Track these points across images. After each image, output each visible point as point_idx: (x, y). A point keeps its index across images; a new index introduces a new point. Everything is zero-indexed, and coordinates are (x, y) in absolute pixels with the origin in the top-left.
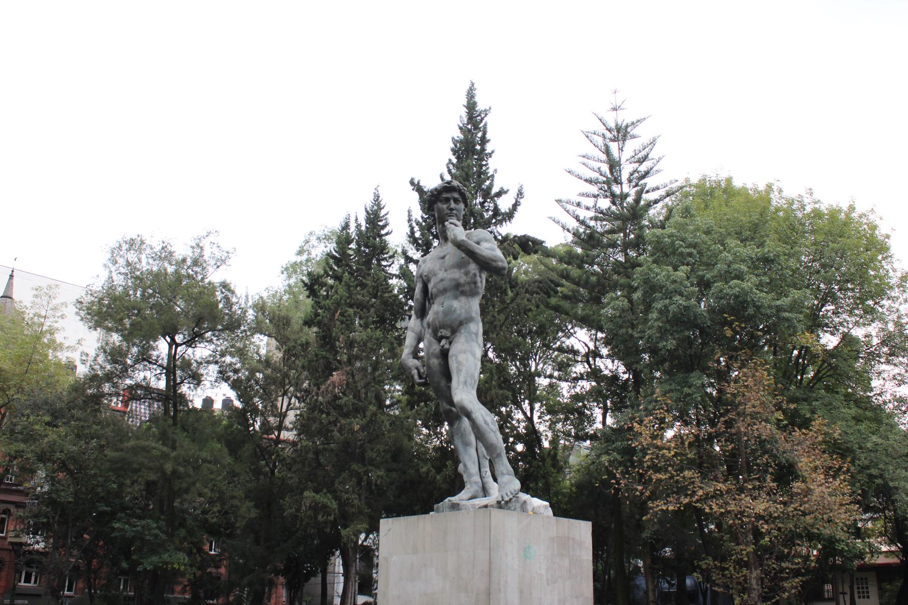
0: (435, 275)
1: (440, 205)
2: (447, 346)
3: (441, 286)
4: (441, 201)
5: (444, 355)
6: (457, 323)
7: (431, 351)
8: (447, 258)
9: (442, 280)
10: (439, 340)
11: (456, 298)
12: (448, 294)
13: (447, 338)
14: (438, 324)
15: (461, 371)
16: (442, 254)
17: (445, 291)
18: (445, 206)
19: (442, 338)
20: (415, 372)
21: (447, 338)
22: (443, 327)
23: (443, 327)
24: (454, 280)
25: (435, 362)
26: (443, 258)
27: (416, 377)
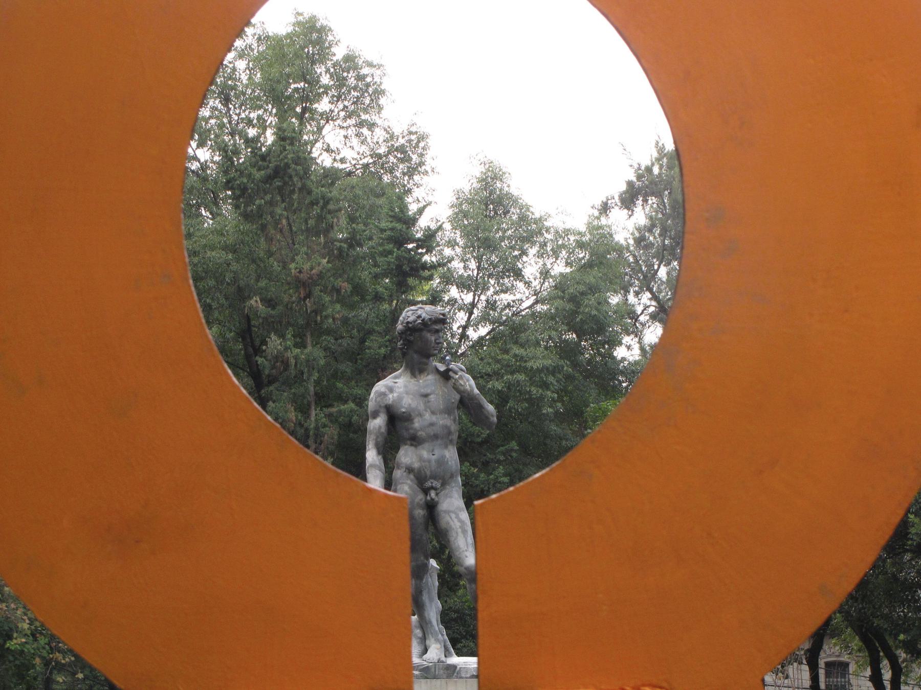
0: (420, 415)
1: (428, 335)
2: (436, 499)
3: (431, 431)
4: (429, 331)
5: (431, 508)
7: (417, 500)
9: (432, 424)
10: (426, 491)
11: (446, 447)
12: (439, 442)
14: (428, 473)
17: (436, 437)
19: (432, 488)
21: (435, 489)
22: (434, 477)
23: (434, 477)
24: (446, 427)
25: (420, 513)
26: (426, 396)
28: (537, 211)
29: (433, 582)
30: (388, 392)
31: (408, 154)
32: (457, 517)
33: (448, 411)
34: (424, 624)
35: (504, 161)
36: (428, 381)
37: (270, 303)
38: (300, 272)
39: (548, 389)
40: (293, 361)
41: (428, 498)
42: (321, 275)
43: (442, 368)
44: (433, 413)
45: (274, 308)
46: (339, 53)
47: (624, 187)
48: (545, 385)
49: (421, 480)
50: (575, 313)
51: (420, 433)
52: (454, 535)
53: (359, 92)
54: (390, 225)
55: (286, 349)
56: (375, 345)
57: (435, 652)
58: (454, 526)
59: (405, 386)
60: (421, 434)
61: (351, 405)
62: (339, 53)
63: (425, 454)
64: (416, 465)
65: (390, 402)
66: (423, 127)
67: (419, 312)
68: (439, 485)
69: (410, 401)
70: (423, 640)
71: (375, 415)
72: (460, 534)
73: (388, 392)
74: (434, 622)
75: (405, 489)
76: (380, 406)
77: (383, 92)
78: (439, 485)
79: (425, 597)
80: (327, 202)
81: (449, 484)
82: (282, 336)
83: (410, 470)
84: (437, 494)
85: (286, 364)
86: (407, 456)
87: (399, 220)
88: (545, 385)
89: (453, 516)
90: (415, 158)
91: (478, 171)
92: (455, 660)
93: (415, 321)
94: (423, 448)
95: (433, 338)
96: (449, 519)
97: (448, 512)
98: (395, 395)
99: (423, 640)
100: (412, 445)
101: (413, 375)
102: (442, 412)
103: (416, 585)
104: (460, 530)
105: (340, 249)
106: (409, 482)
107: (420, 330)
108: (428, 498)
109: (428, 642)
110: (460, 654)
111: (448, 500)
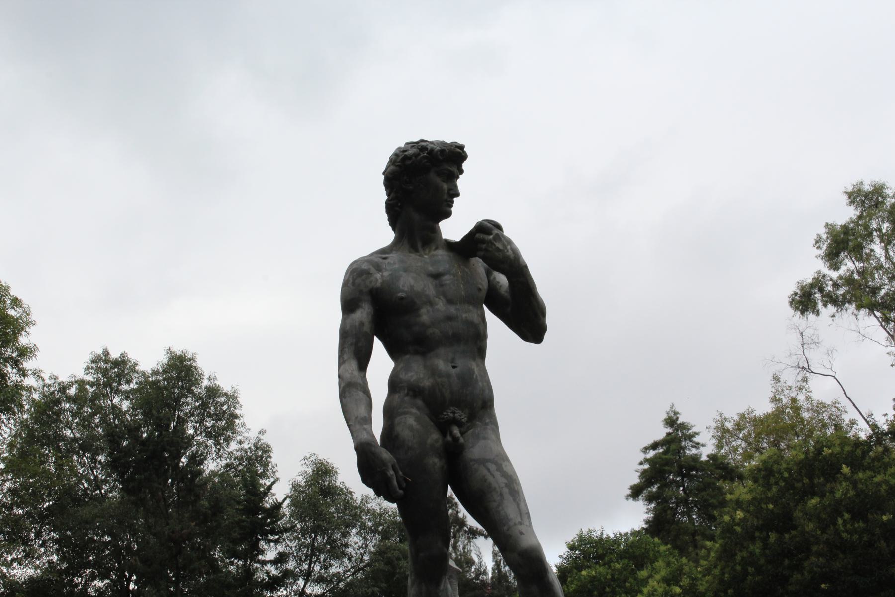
4: (439, 174)
7: (429, 441)
8: (447, 278)
9: (450, 318)
10: (443, 427)
11: (474, 359)
13: (459, 424)
16: (430, 268)
18: (445, 186)
20: (391, 472)
21: (459, 424)
23: (458, 402)
25: (435, 462)
26: (436, 276)
27: (395, 482)
30: (373, 270)
38: (173, 532)
44: (450, 302)
46: (205, 383)
51: (430, 331)
52: (497, 498)
53: (220, 413)
58: (494, 484)
59: (402, 261)
60: (435, 331)
62: (205, 383)
63: (441, 365)
64: (427, 383)
65: (379, 284)
66: (265, 439)
68: (465, 420)
69: (412, 282)
73: (373, 270)
76: (361, 291)
77: (236, 417)
78: (465, 420)
83: (415, 391)
89: (492, 467)
93: (416, 155)
96: (485, 472)
97: (483, 461)
100: (416, 353)
101: (414, 248)
104: (505, 490)
106: (414, 411)
108: (449, 438)
111: (481, 443)
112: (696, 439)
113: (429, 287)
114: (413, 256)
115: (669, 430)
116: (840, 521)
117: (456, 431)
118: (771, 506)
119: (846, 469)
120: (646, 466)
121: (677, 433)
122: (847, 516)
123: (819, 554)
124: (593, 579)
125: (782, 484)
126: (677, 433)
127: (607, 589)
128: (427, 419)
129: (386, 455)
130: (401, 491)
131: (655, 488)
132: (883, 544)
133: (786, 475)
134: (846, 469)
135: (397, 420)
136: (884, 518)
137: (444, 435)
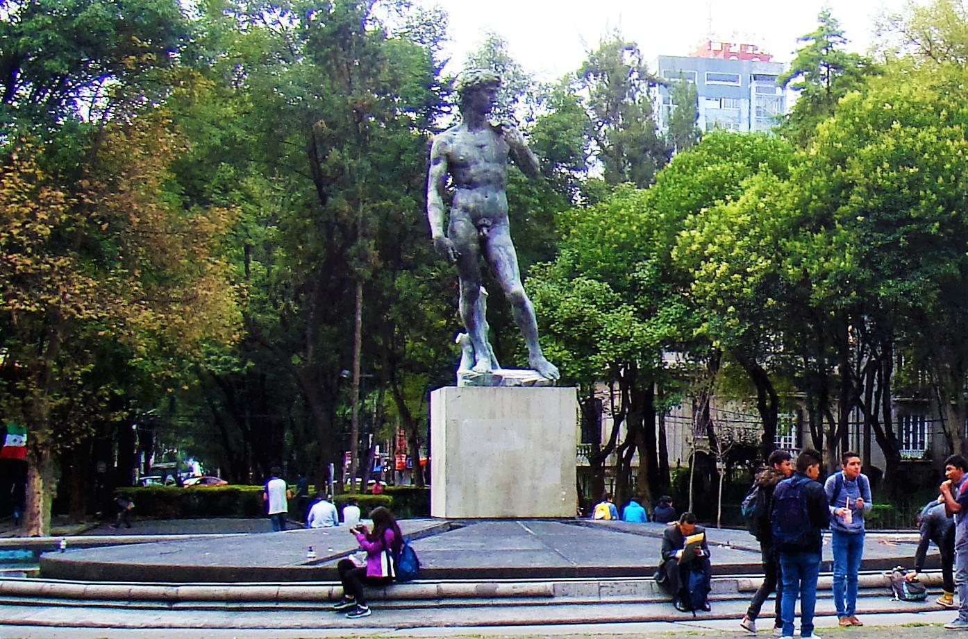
0: (476, 163)
1: (484, 95)
5: (484, 242)
6: (499, 215)
9: (486, 171)
10: (479, 228)
11: (497, 191)
12: (491, 186)
13: (487, 226)
15: (513, 263)
17: (489, 182)
21: (487, 226)
22: (487, 216)
23: (487, 216)
25: (474, 246)
26: (481, 146)
27: (452, 256)
28: (526, 70)
29: (483, 306)
30: (448, 142)
31: (433, 28)
32: (505, 250)
33: (499, 160)
34: (474, 342)
35: (503, 33)
36: (484, 135)
37: (332, 125)
39: (531, 196)
40: (347, 168)
41: (481, 234)
42: (370, 106)
43: (495, 123)
44: (487, 161)
45: (334, 129)
47: (581, 66)
48: (530, 194)
49: (476, 218)
50: (553, 144)
51: (474, 178)
52: (503, 265)
54: (421, 73)
55: (343, 158)
56: (408, 159)
57: (483, 365)
61: (390, 202)
64: (471, 205)
65: (450, 151)
66: (446, 8)
67: (477, 75)
70: (473, 355)
71: (436, 162)
72: (508, 266)
73: (448, 142)
74: (483, 340)
75: (462, 225)
78: (490, 224)
79: (476, 318)
80: (376, 53)
81: (500, 223)
82: (341, 149)
83: (465, 209)
84: (488, 231)
85: (342, 169)
86: (464, 198)
87: (428, 69)
88: (530, 194)
89: (502, 249)
90: (439, 32)
91: (484, 39)
92: (499, 372)
94: (477, 191)
95: (489, 97)
97: (498, 247)
98: (455, 145)
99: (473, 355)
100: (468, 188)
101: (470, 129)
102: (495, 161)
103: (469, 307)
104: (507, 262)
105: (384, 88)
106: (465, 219)
107: (479, 90)
109: (477, 356)
110: (503, 368)
112: (844, 35)
113: (475, 153)
114: (470, 134)
115: (823, 24)
116: (879, 170)
117: (485, 230)
118: (840, 145)
119: (896, 125)
120: (796, 56)
121: (829, 30)
122: (886, 165)
123: (860, 194)
124: (717, 174)
125: (852, 127)
126: (829, 30)
127: (726, 185)
128: (471, 224)
129: (448, 241)
130: (455, 260)
131: (800, 79)
132: (905, 191)
133: (857, 120)
134: (896, 125)
135: (455, 223)
136: (911, 170)
137: (479, 231)
